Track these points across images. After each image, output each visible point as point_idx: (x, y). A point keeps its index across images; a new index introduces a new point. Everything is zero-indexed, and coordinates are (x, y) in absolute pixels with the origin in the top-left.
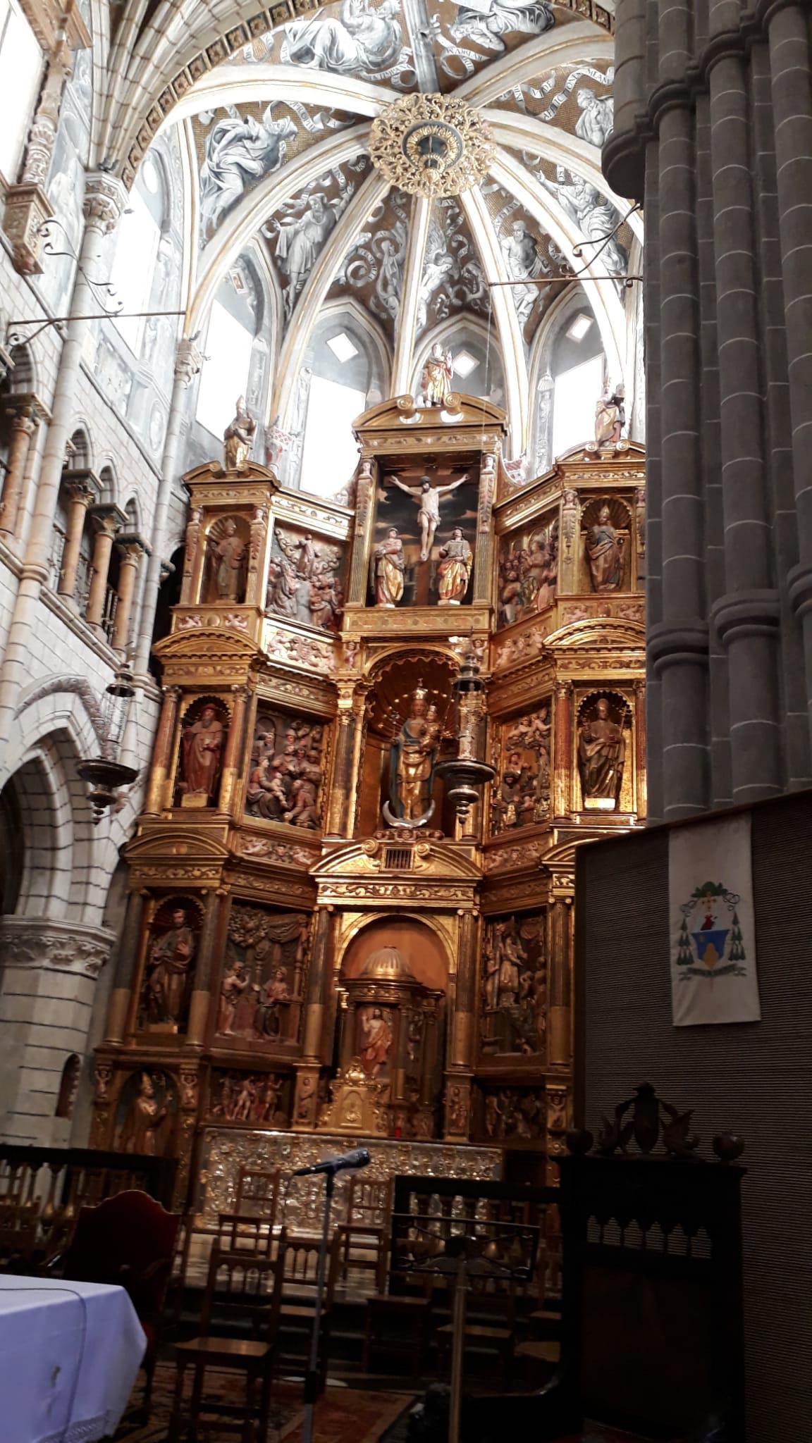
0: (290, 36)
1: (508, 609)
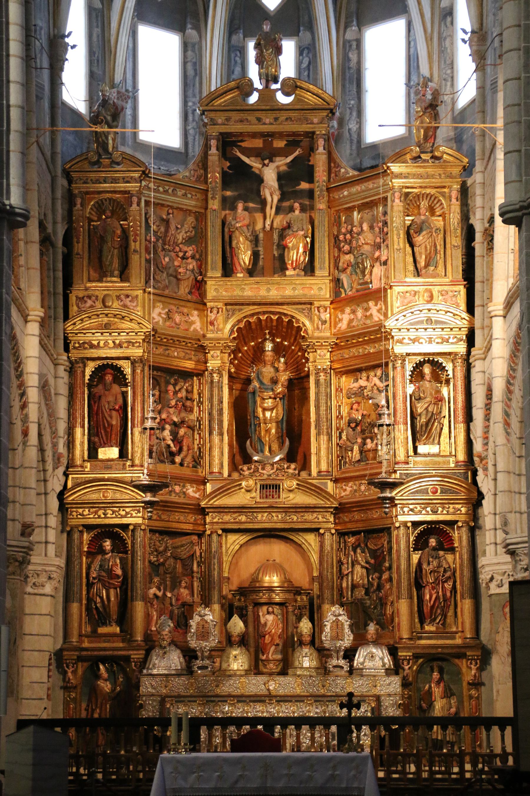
1: (344, 278)
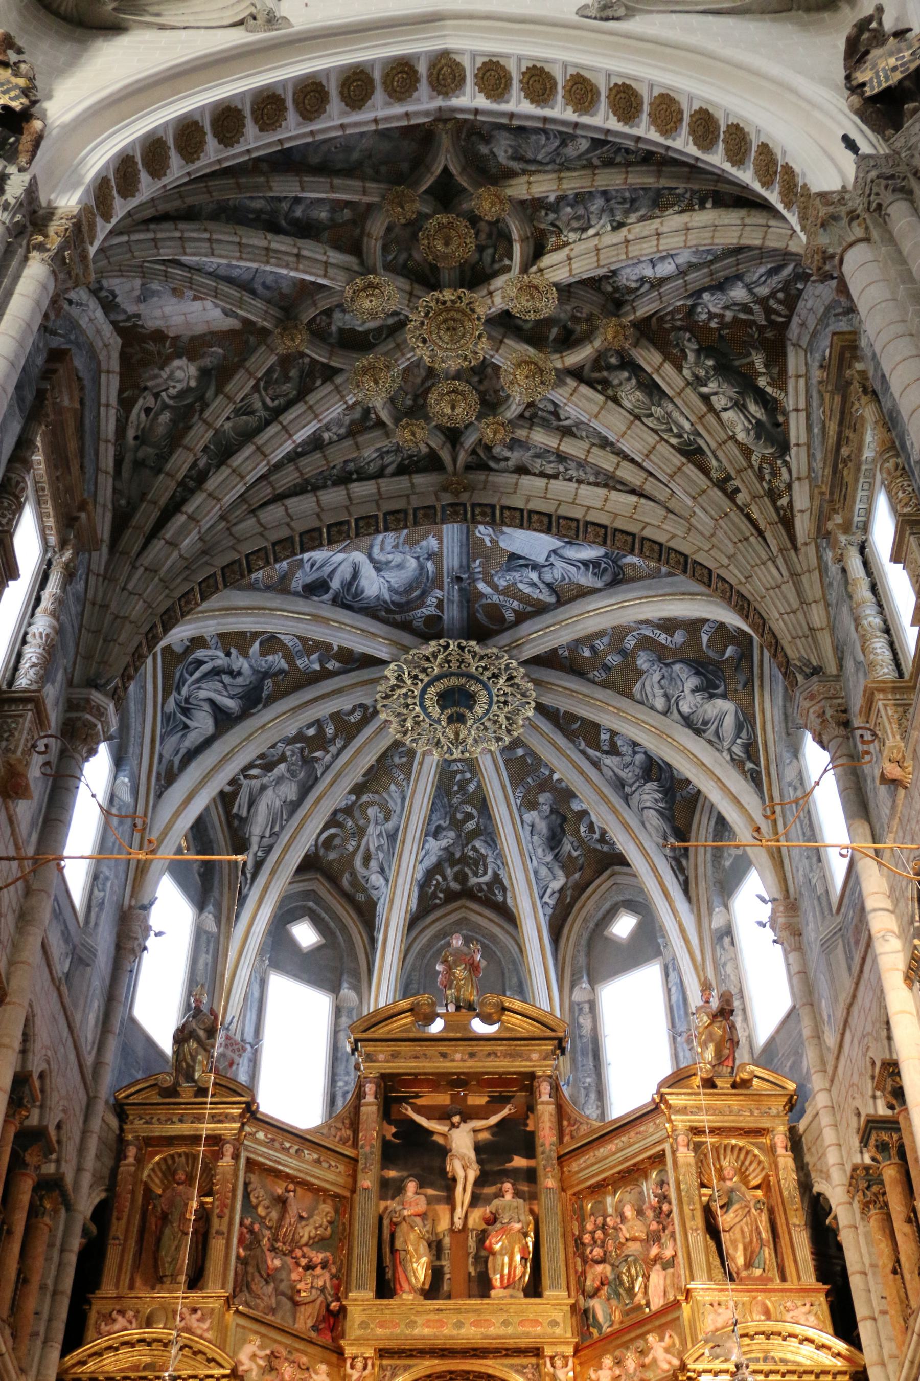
0: (307, 567)
1: (597, 1306)
